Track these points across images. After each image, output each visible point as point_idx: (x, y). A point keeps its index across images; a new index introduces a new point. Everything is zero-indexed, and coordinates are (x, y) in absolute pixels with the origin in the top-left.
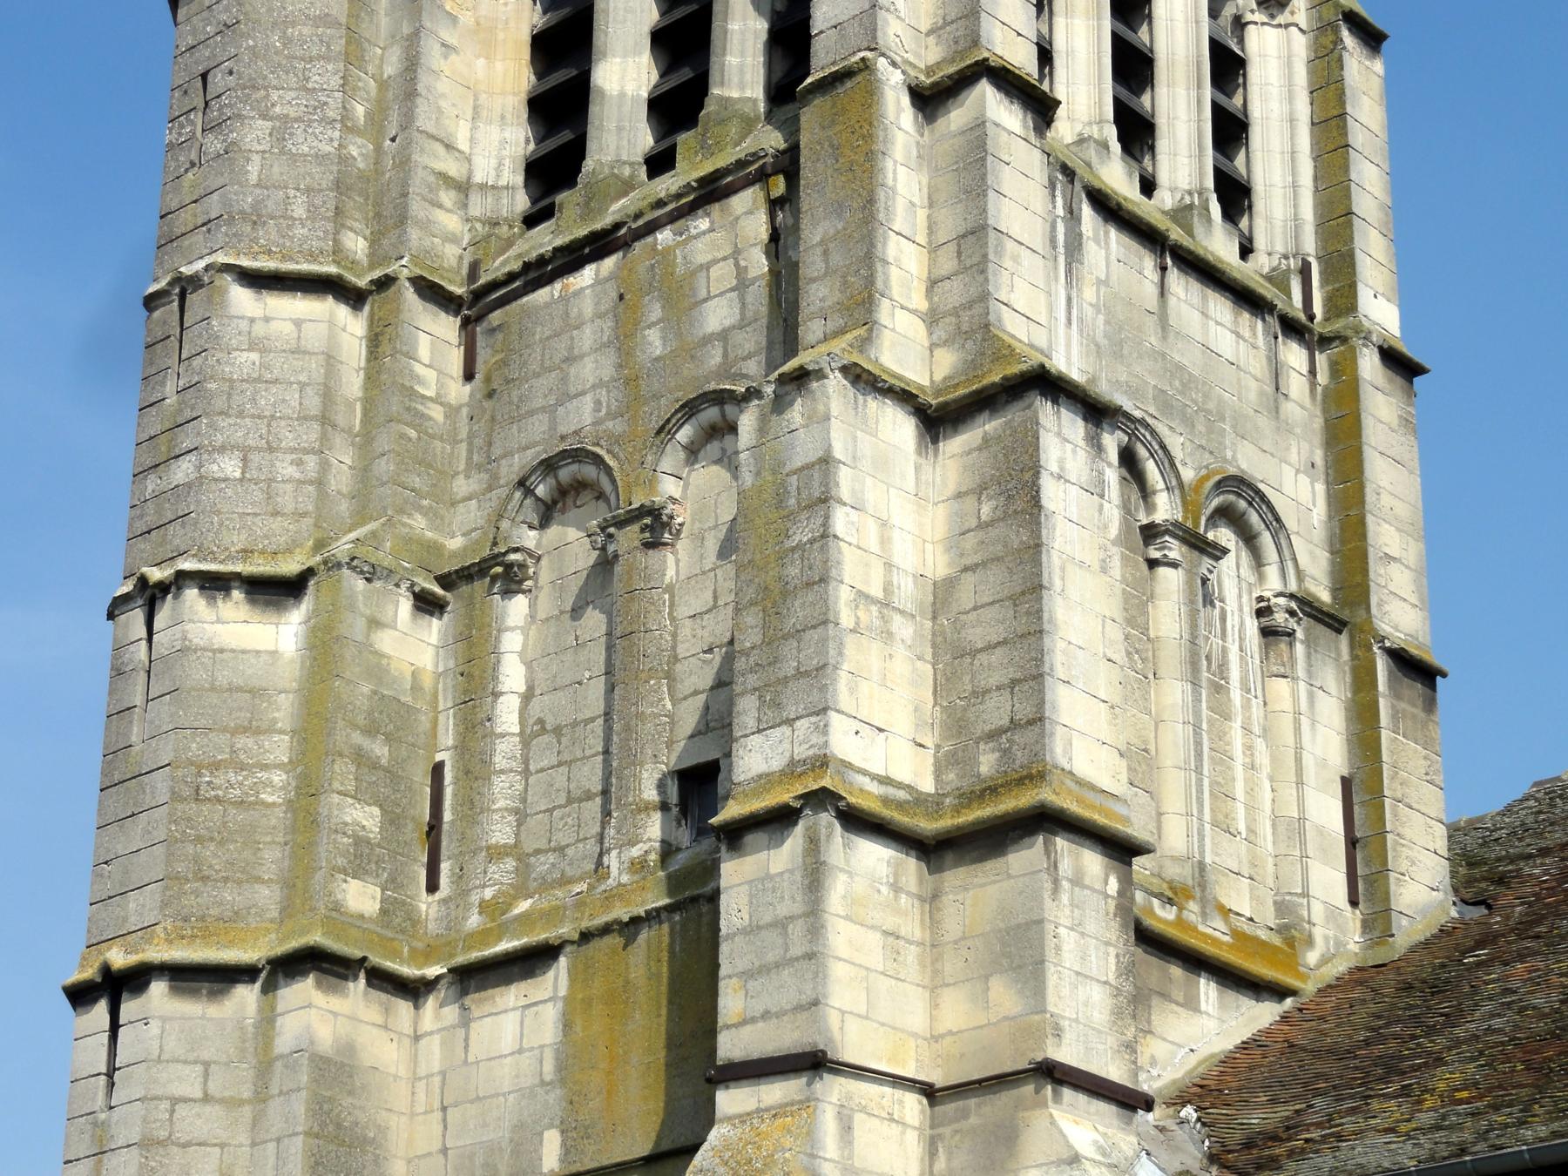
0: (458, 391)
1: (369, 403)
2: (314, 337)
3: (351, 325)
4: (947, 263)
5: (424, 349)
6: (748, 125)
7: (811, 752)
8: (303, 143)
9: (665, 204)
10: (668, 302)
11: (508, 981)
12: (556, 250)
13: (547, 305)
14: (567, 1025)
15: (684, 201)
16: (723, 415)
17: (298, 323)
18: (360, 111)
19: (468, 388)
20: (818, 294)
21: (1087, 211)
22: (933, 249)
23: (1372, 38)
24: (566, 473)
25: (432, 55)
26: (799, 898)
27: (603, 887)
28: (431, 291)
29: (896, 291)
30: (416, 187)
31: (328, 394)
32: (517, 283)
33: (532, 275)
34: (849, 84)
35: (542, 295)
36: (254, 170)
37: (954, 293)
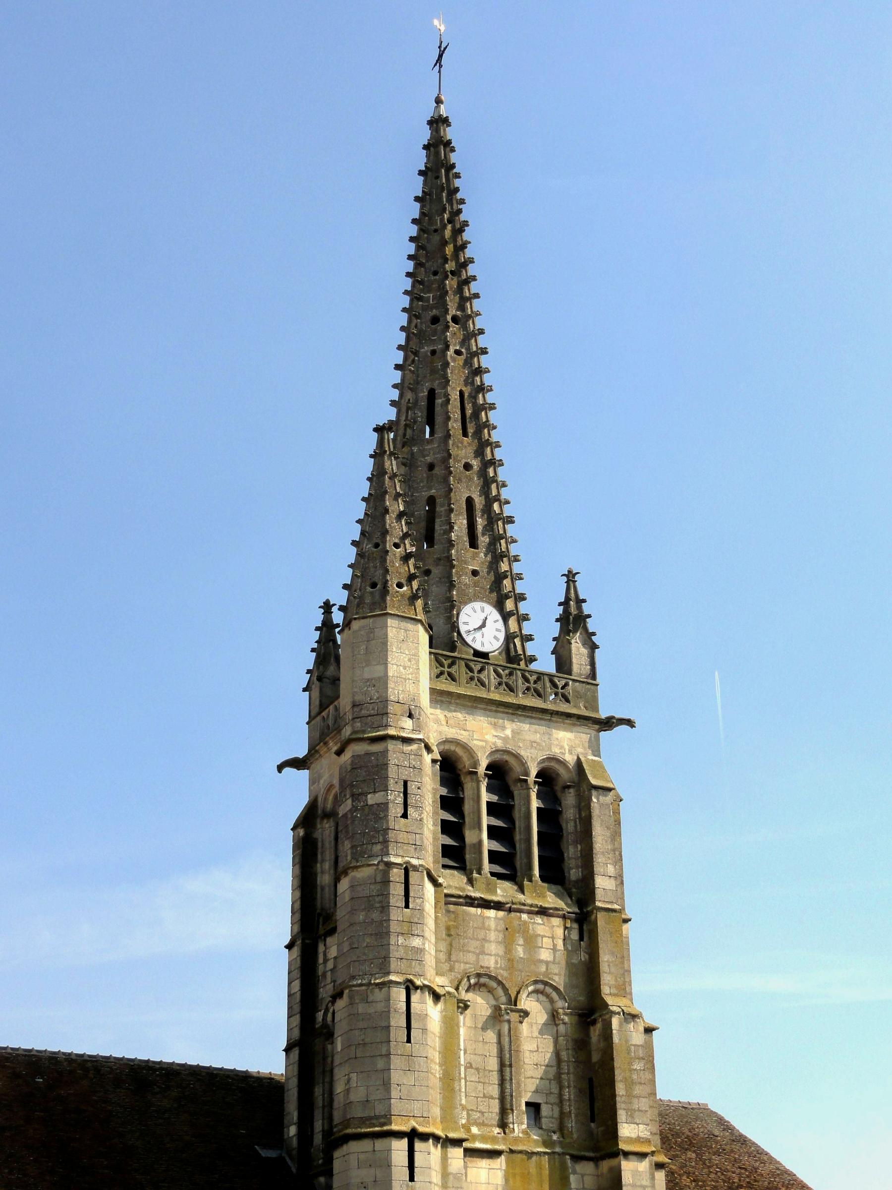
7: (645, 1136)
10: (526, 940)
11: (483, 1157)
14: (507, 1180)
15: (533, 909)
24: (483, 980)
26: (648, 1181)
27: (512, 1135)
32: (461, 900)
34: (614, 914)
35: (472, 910)
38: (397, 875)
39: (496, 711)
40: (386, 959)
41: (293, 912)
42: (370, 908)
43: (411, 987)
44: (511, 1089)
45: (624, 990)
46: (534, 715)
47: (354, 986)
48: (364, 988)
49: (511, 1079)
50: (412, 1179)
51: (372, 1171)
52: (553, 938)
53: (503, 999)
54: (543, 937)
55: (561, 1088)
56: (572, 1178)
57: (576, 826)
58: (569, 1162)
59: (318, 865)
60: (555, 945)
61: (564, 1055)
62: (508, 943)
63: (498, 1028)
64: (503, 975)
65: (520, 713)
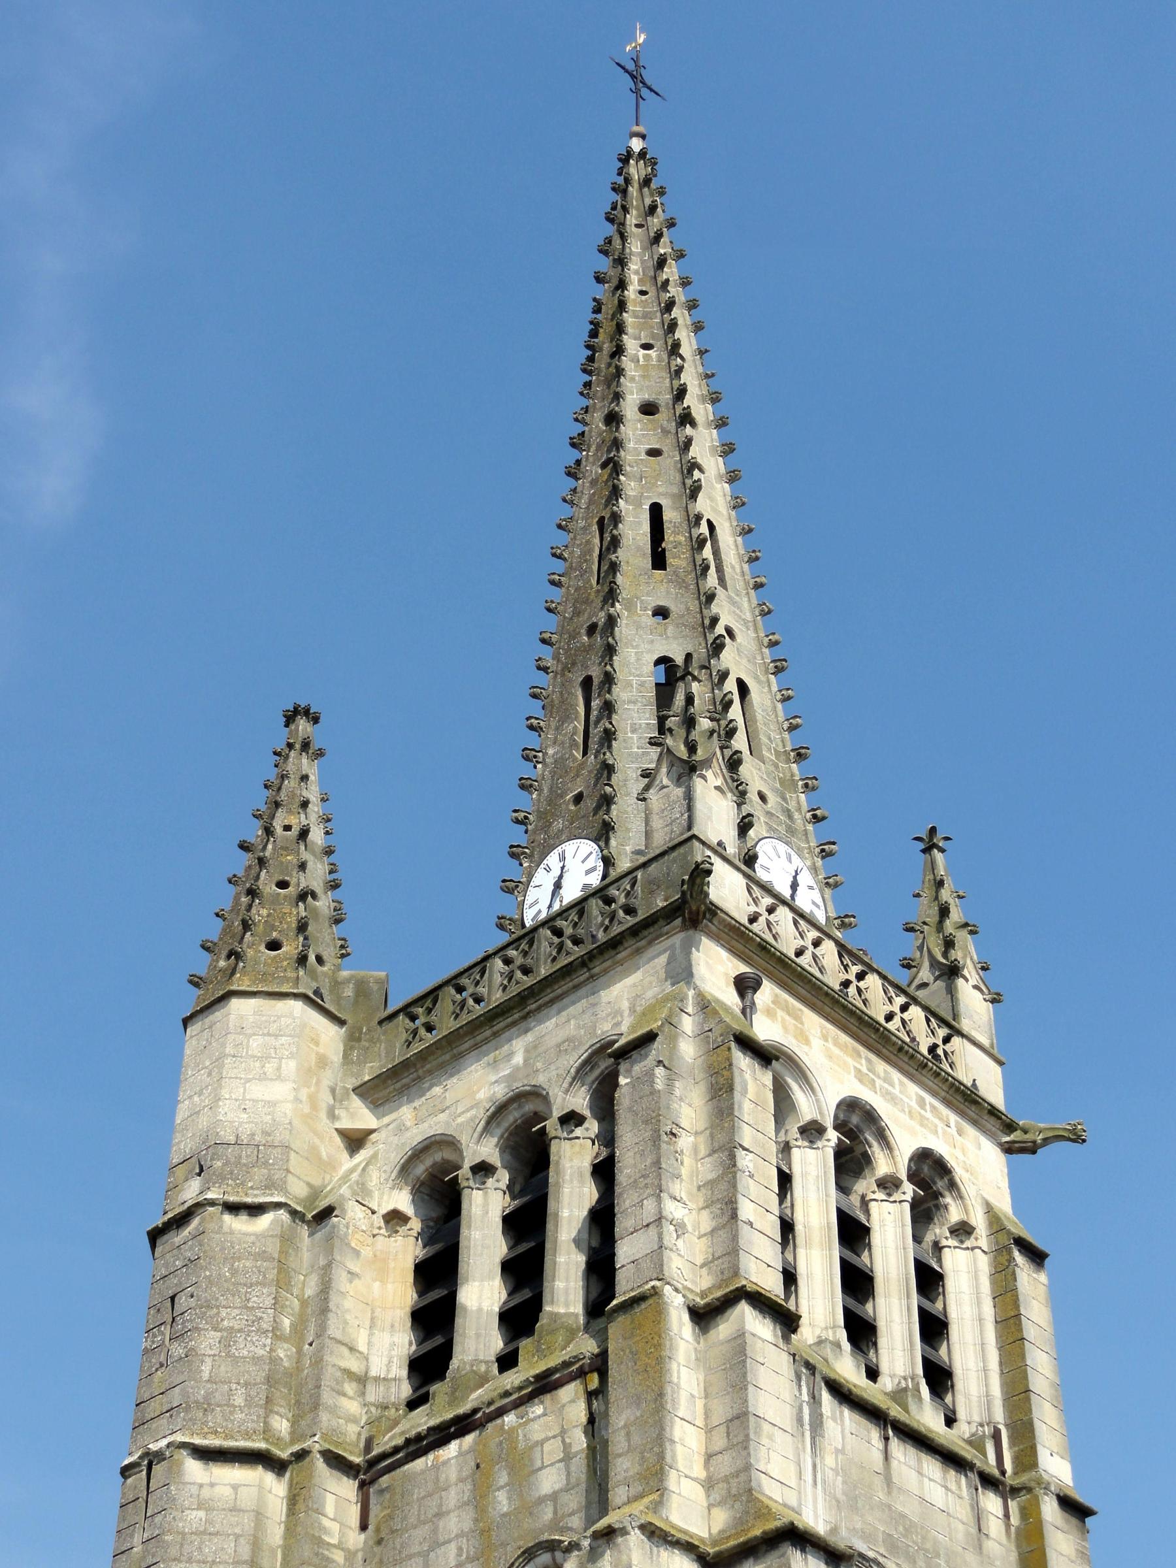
0: (356, 1539)
1: (287, 1549)
2: (247, 1498)
3: (275, 1488)
4: (720, 1442)
5: (330, 1508)
6: (572, 1334)
8: (243, 1349)
9: (511, 1394)
10: (512, 1470)
12: (429, 1429)
13: (423, 1472)
16: (554, 1559)
17: (235, 1487)
18: (286, 1323)
19: (363, 1536)
20: (623, 1467)
21: (826, 1396)
22: (709, 1430)
23: (1037, 1257)
25: (341, 1280)
28: (336, 1461)
29: (681, 1464)
30: (327, 1381)
31: (256, 1544)
32: (401, 1455)
33: (412, 1448)
34: (643, 1306)
35: (419, 1464)
36: (206, 1369)
37: (725, 1464)
39: (496, 1035)
46: (559, 991)
65: (534, 1006)
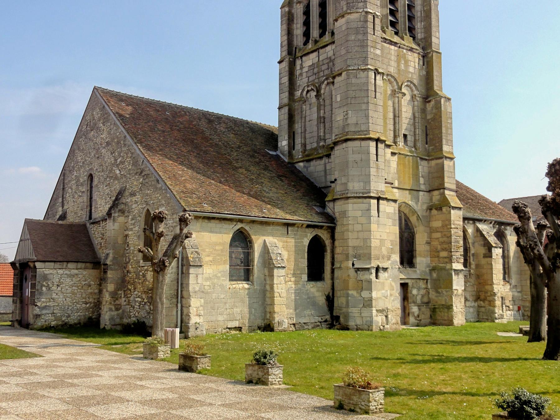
14: (398, 166)
38: (370, 17)
40: (366, 58)
41: (282, 47)
42: (357, 33)
43: (376, 73)
44: (399, 127)
45: (441, 89)
47: (350, 70)
48: (355, 71)
49: (399, 123)
50: (377, 160)
51: (360, 155)
52: (414, 62)
53: (396, 87)
54: (411, 61)
55: (415, 129)
56: (420, 167)
57: (421, 14)
58: (419, 160)
59: (295, 25)
60: (415, 66)
61: (417, 115)
62: (398, 62)
63: (393, 100)
64: (396, 76)
